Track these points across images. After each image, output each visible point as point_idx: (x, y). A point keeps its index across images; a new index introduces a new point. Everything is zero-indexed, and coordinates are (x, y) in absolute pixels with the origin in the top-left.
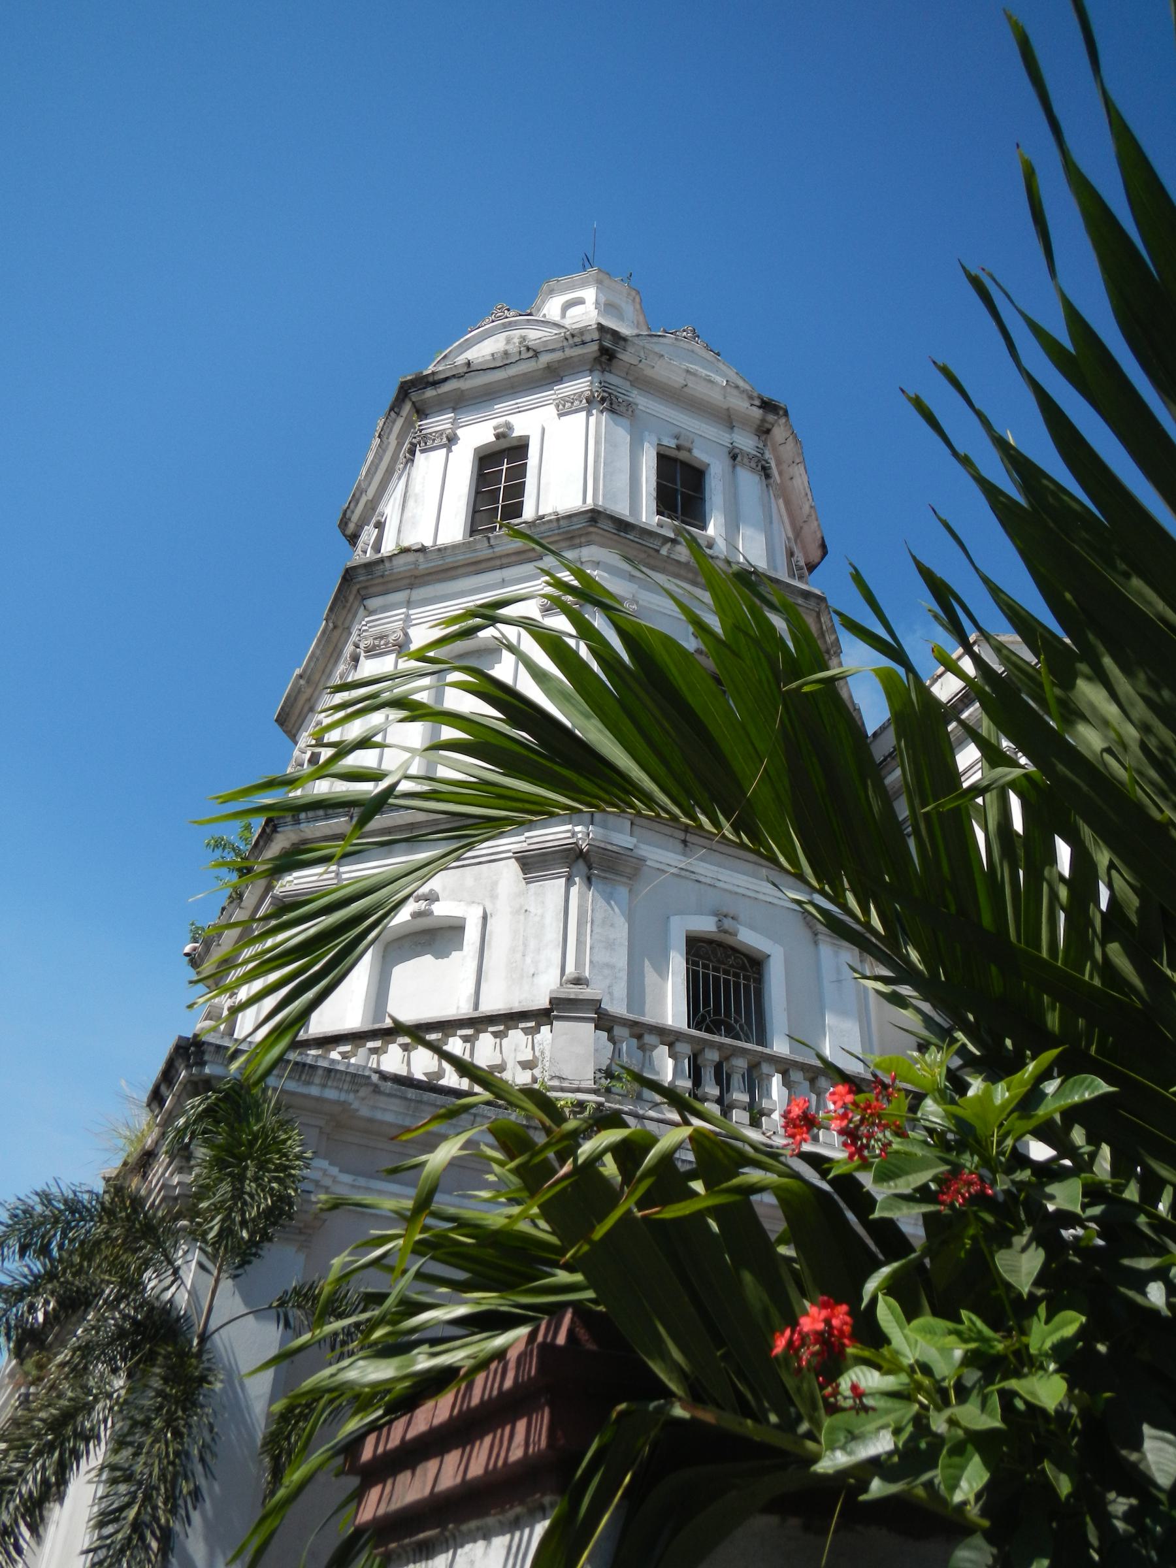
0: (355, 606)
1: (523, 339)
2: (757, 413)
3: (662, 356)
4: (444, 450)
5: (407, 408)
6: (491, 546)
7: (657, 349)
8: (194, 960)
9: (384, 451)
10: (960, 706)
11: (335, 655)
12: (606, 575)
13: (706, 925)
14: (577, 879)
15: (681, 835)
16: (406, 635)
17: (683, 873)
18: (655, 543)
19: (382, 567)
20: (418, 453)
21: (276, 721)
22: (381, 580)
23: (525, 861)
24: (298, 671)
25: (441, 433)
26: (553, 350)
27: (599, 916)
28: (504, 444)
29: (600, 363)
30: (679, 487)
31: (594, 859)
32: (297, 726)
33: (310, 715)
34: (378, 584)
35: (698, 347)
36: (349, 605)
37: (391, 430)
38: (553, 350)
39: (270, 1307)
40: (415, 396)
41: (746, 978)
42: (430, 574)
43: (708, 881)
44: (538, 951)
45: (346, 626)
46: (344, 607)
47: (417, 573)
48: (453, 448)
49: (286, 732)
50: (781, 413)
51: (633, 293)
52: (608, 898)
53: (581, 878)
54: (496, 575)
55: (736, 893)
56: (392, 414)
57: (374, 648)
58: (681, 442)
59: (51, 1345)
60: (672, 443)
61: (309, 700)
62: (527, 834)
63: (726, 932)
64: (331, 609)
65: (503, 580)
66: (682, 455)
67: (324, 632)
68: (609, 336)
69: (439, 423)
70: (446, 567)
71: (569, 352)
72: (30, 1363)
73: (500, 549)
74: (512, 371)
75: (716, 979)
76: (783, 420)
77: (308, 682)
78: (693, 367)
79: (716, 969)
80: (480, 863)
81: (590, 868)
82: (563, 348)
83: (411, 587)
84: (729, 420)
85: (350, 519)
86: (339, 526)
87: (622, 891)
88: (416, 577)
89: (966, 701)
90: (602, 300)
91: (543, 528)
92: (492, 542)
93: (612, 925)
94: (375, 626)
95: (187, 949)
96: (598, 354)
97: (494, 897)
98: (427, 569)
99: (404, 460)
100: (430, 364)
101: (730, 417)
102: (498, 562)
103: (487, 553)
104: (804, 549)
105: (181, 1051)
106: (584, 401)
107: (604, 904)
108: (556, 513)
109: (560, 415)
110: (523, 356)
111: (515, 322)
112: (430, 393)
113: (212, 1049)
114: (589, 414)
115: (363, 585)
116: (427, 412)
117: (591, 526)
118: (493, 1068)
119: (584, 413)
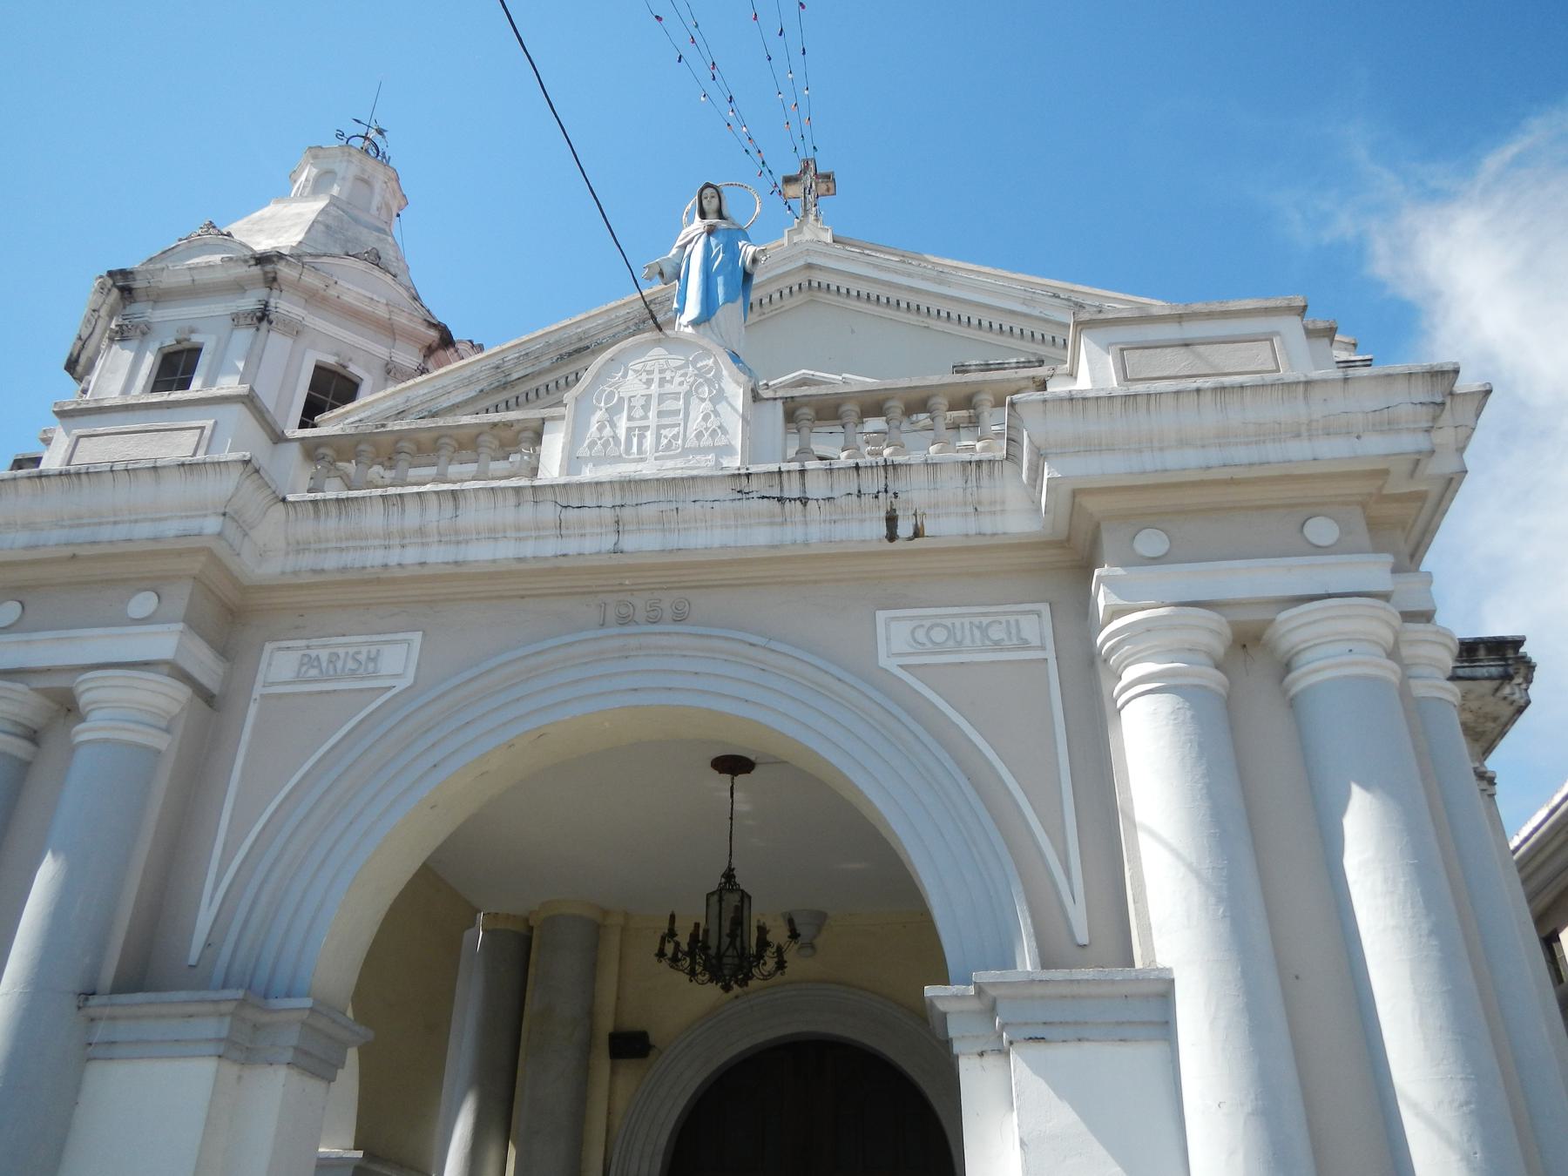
2: (256, 270)
7: (158, 266)
38: (102, 305)
51: (346, 149)
58: (181, 337)
66: (185, 345)
68: (119, 277)
82: (104, 302)
84: (239, 287)
90: (315, 171)
96: (120, 294)
104: (410, 336)
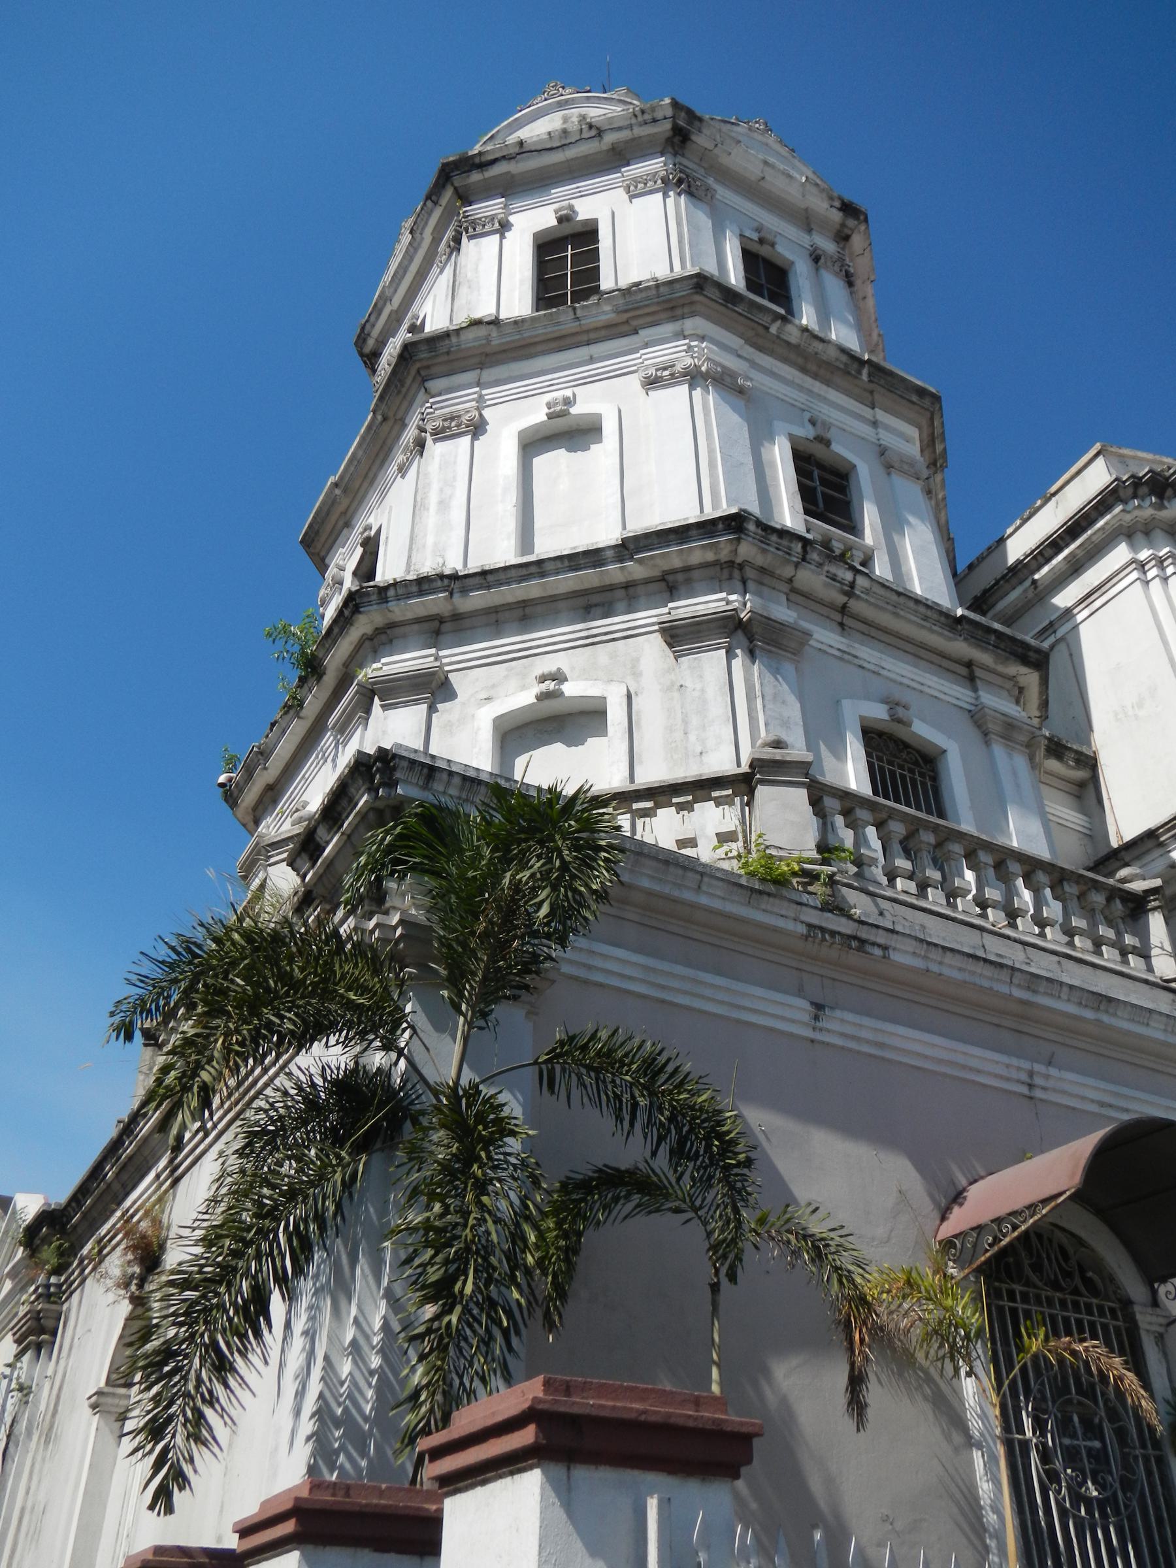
0: (412, 392)
1: (583, 118)
2: (836, 216)
3: (739, 142)
4: (498, 236)
5: (448, 194)
6: (578, 319)
8: (230, 794)
9: (416, 250)
10: (1094, 514)
11: (381, 456)
12: (715, 348)
13: (878, 712)
14: (738, 651)
15: (838, 617)
16: (481, 415)
17: (846, 657)
18: (765, 319)
19: (447, 342)
20: (464, 239)
21: (301, 542)
22: (445, 358)
23: (674, 632)
24: (332, 479)
25: (492, 219)
26: (620, 129)
27: (769, 691)
28: (567, 229)
29: (673, 145)
30: (763, 281)
31: (756, 629)
32: (327, 546)
33: (345, 531)
34: (440, 363)
35: (771, 139)
36: (404, 390)
37: (426, 223)
38: (620, 129)
39: (536, 1063)
40: (458, 181)
41: (922, 775)
42: (504, 351)
43: (872, 667)
44: (704, 728)
45: (398, 417)
46: (399, 392)
47: (488, 350)
48: (507, 234)
49: (310, 555)
50: (862, 218)
52: (776, 672)
53: (743, 650)
54: (583, 352)
55: (901, 684)
56: (429, 203)
57: (444, 429)
58: (763, 234)
59: (75, 1227)
60: (755, 236)
61: (344, 513)
62: (671, 605)
63: (900, 721)
64: (381, 398)
65: (591, 358)
67: (369, 427)
68: (683, 114)
69: (490, 208)
70: (522, 343)
71: (638, 131)
72: (49, 1254)
73: (588, 321)
74: (571, 153)
75: (893, 773)
76: (863, 227)
77: (345, 491)
78: (772, 160)
79: (890, 763)
80: (614, 640)
81: (751, 639)
82: (631, 127)
83: (481, 366)
84: (807, 221)
85: (369, 335)
86: (356, 344)
87: (789, 667)
88: (487, 355)
89: (1101, 508)
91: (640, 296)
92: (579, 313)
93: (784, 702)
94: (442, 408)
95: (222, 779)
96: (670, 134)
97: (636, 674)
98: (500, 345)
99: (448, 250)
100: (475, 145)
101: (807, 218)
102: (585, 338)
103: (572, 327)
105: (363, 769)
106: (659, 181)
107: (772, 679)
108: (655, 279)
109: (632, 197)
110: (585, 135)
111: (573, 99)
112: (476, 177)
113: (405, 764)
114: (666, 196)
115: (425, 363)
116: (472, 199)
117: (697, 293)
118: (682, 843)
119: (660, 195)
